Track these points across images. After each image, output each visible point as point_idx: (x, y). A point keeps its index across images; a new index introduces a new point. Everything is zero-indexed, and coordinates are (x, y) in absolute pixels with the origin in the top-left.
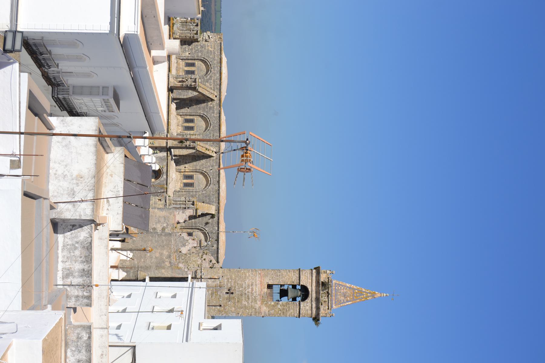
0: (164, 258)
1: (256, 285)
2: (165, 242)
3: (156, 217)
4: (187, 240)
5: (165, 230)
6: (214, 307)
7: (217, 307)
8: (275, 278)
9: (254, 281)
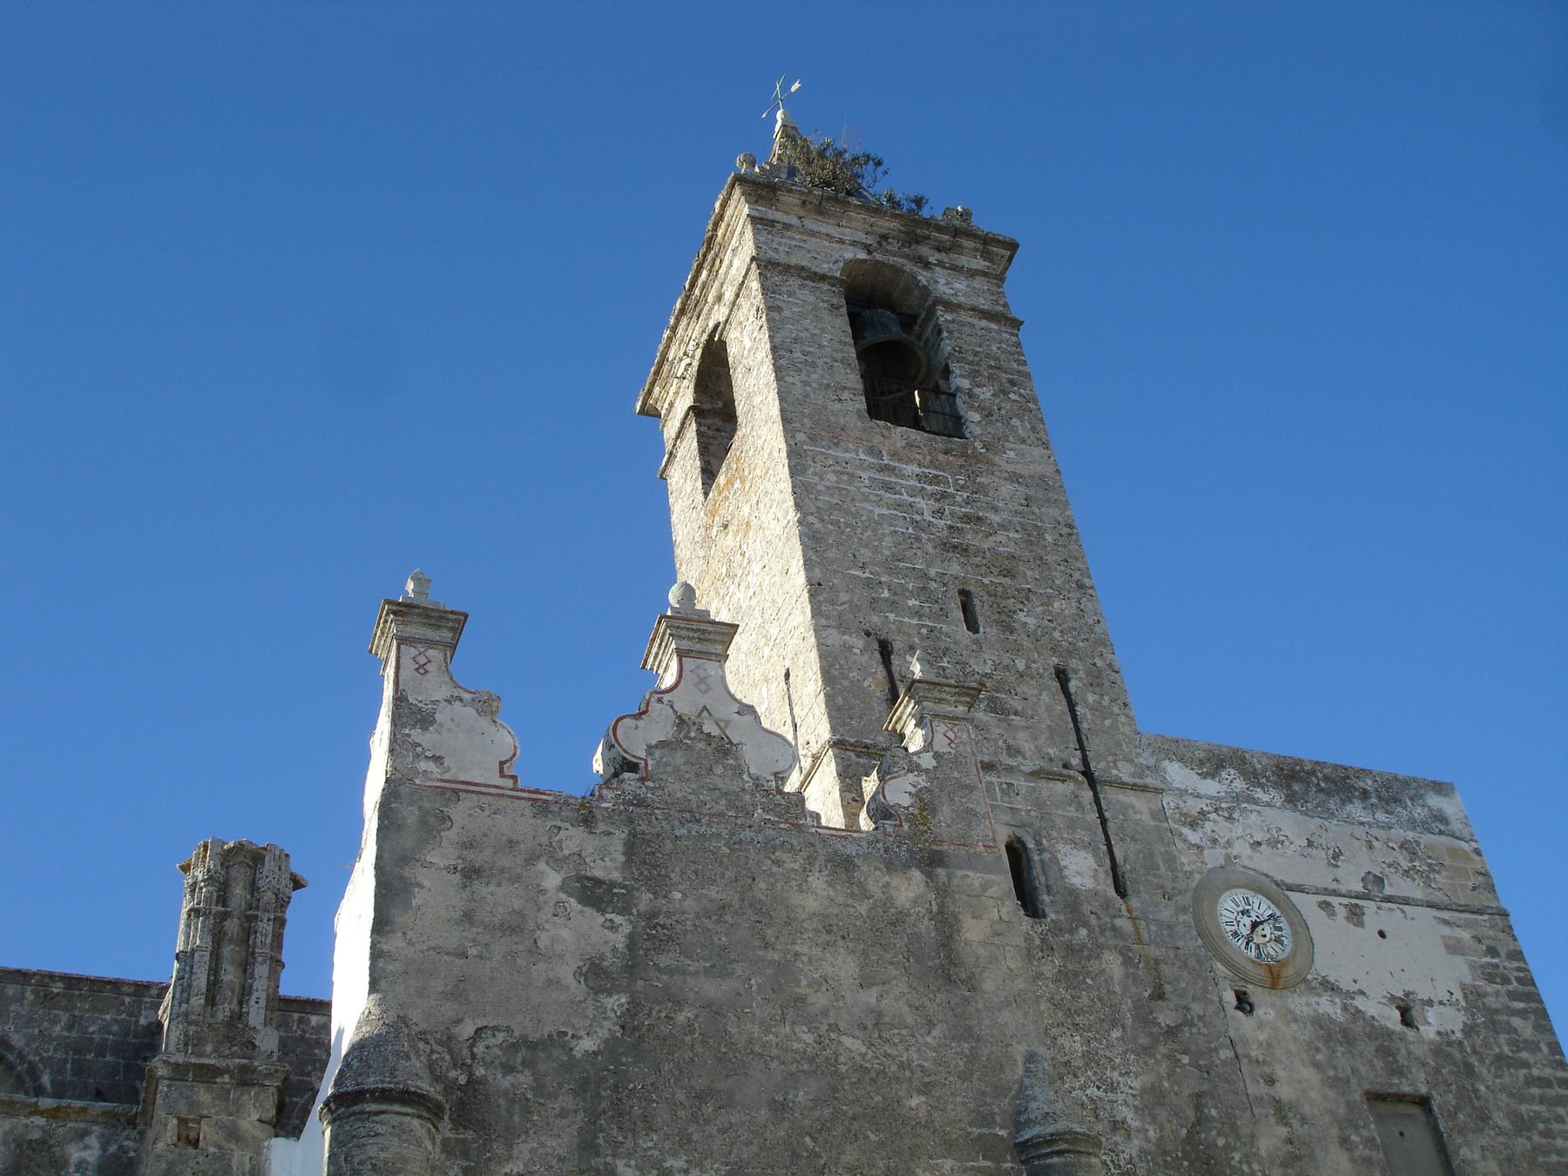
0: (863, 908)
1: (884, 469)
2: (713, 892)
3: (473, 952)
4: (681, 722)
5: (598, 882)
6: (1078, 708)
7: (1072, 690)
8: (822, 376)
9: (864, 475)
